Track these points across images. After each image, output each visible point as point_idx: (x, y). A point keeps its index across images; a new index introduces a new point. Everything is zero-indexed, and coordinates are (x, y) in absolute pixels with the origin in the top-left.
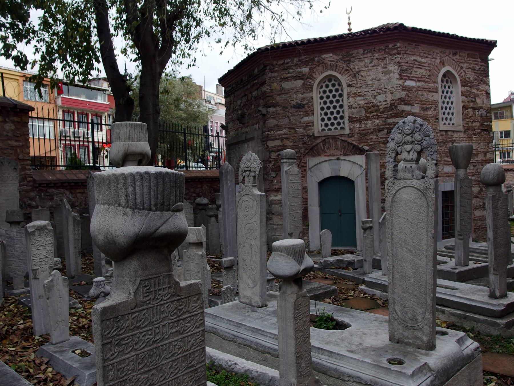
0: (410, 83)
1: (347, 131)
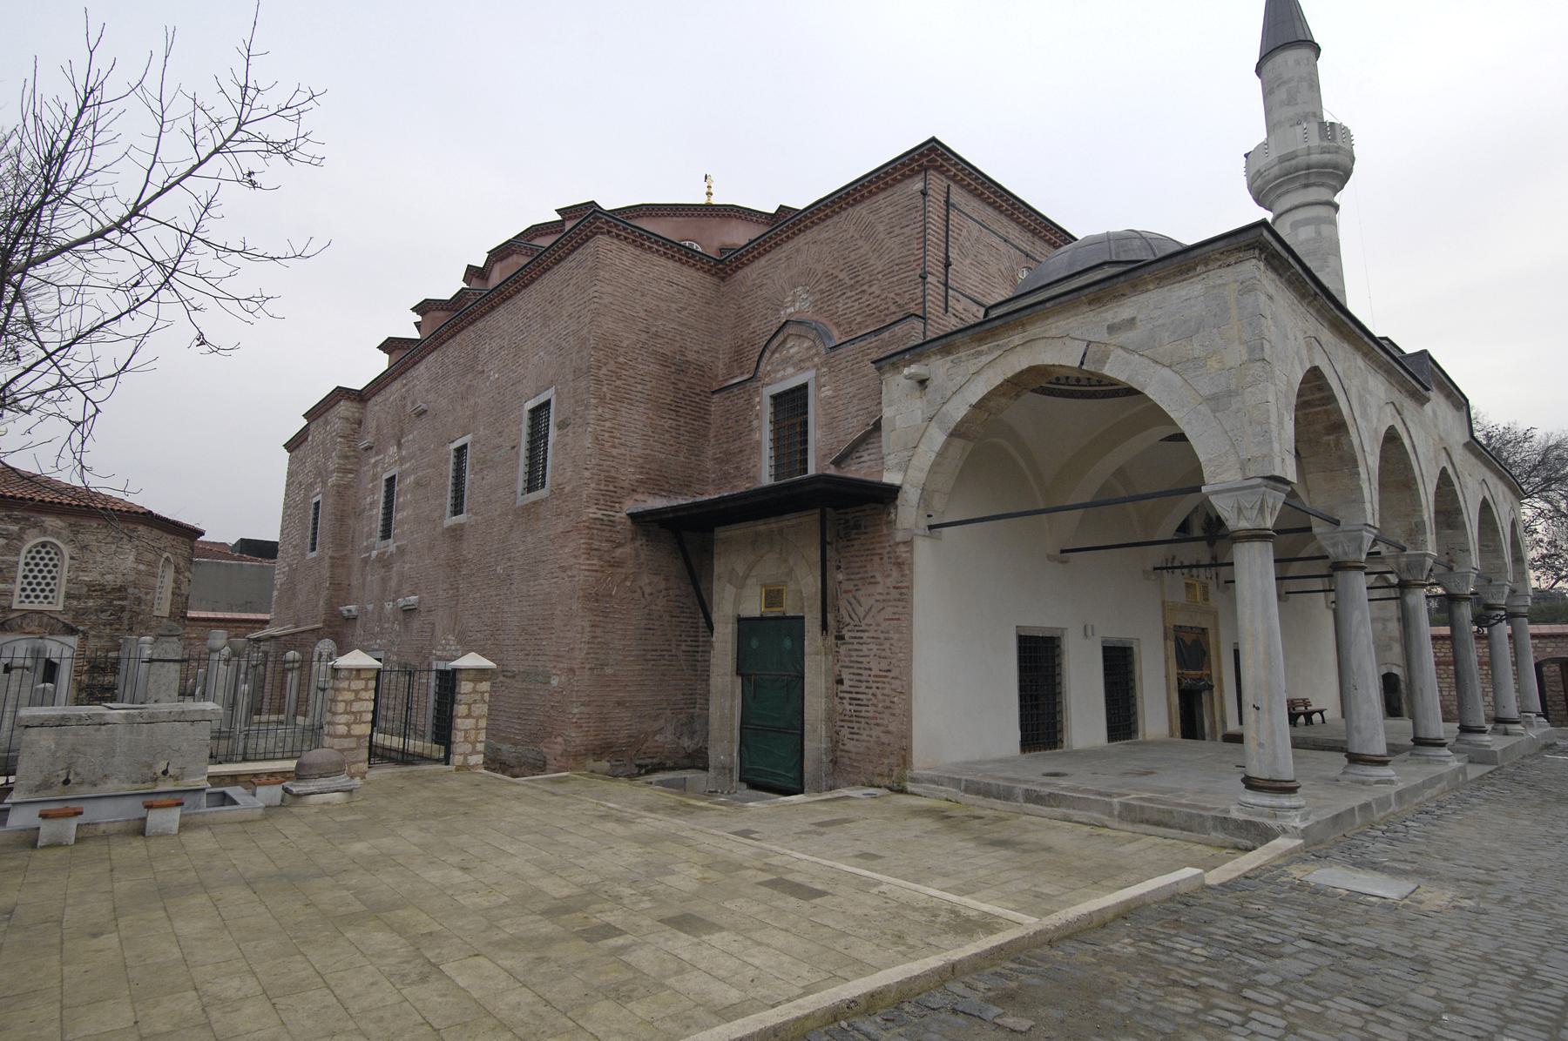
0: (142, 567)
1: (60, 607)
